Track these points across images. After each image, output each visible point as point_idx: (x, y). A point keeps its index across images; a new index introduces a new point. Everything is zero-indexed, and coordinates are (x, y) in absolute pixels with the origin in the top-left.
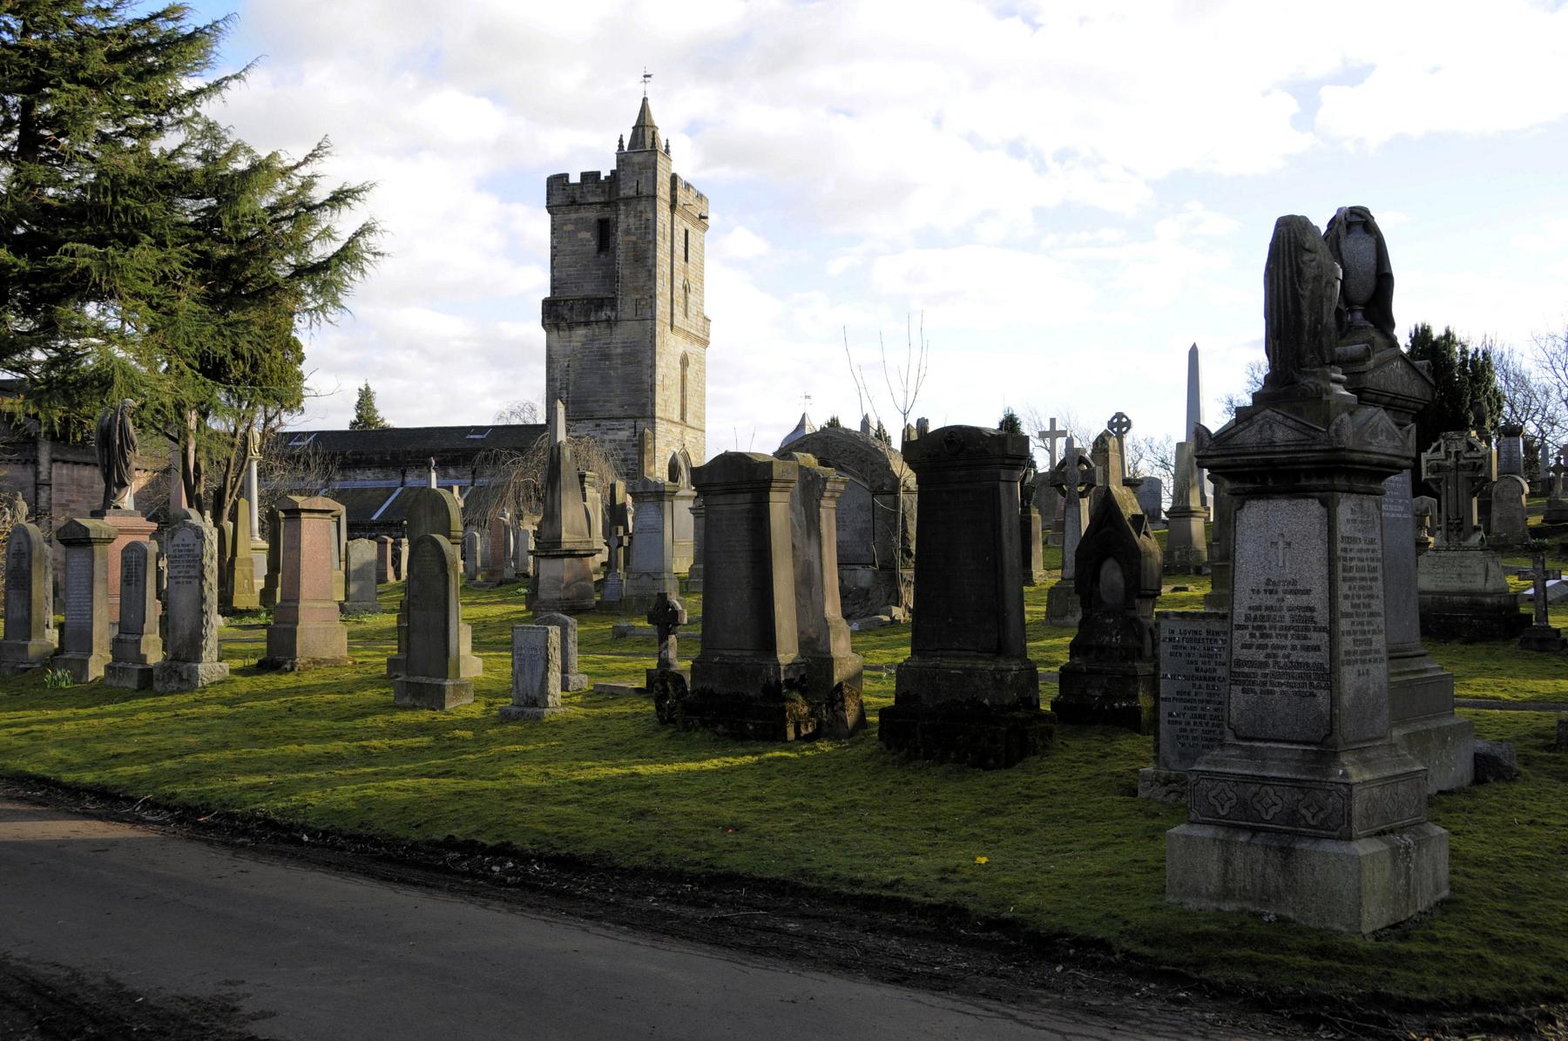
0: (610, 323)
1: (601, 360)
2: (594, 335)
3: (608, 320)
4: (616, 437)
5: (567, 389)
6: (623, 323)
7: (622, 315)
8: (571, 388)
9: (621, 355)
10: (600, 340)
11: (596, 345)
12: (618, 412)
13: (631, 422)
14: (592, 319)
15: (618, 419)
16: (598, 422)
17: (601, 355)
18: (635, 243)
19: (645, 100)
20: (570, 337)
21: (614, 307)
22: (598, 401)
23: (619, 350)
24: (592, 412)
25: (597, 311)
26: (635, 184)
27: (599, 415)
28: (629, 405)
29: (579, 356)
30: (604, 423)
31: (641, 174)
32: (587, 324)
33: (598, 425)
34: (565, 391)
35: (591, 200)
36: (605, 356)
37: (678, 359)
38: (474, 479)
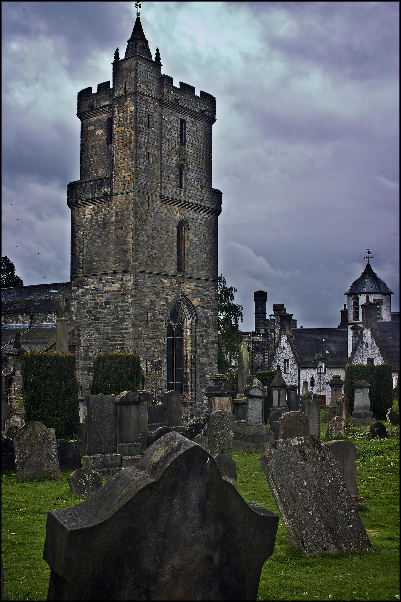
0: (108, 198)
1: (102, 227)
2: (98, 208)
3: (105, 195)
4: (111, 289)
5: (82, 252)
6: (116, 197)
7: (115, 191)
8: (85, 251)
9: (115, 222)
10: (102, 211)
11: (100, 215)
12: (112, 268)
13: (119, 276)
14: (96, 195)
15: (113, 274)
16: (100, 277)
17: (103, 224)
18: (123, 132)
19: (138, 20)
20: (85, 211)
21: (110, 185)
22: (100, 261)
23: (113, 219)
24: (97, 269)
25: (99, 189)
26: (123, 86)
27: (101, 271)
28: (119, 262)
29: (90, 225)
30: (104, 277)
31: (127, 76)
32: (93, 200)
33: (100, 280)
34: (81, 254)
35: (103, 104)
36: (105, 224)
37: (176, 224)
38: (31, 323)
